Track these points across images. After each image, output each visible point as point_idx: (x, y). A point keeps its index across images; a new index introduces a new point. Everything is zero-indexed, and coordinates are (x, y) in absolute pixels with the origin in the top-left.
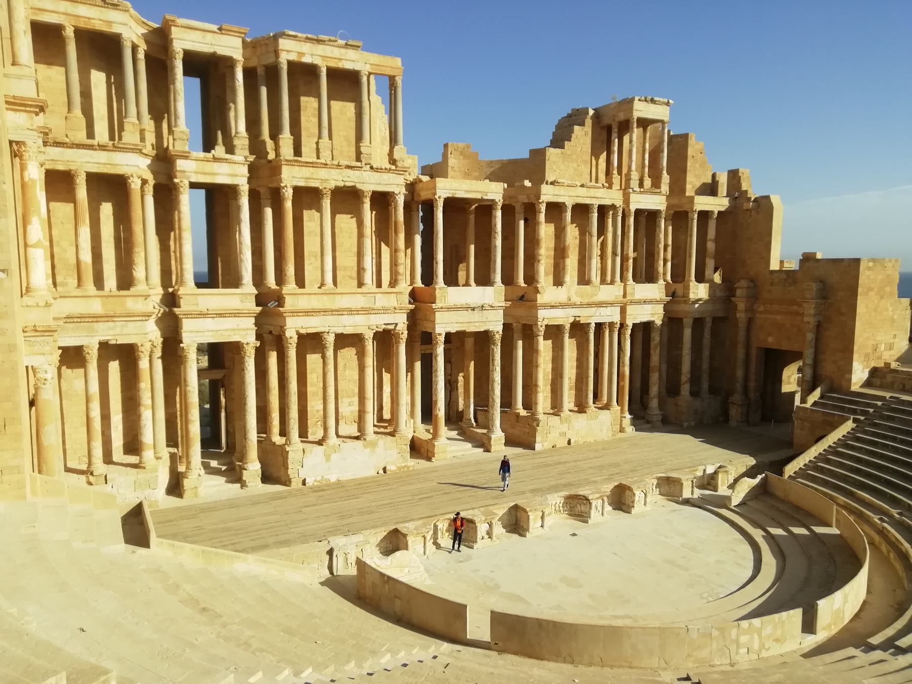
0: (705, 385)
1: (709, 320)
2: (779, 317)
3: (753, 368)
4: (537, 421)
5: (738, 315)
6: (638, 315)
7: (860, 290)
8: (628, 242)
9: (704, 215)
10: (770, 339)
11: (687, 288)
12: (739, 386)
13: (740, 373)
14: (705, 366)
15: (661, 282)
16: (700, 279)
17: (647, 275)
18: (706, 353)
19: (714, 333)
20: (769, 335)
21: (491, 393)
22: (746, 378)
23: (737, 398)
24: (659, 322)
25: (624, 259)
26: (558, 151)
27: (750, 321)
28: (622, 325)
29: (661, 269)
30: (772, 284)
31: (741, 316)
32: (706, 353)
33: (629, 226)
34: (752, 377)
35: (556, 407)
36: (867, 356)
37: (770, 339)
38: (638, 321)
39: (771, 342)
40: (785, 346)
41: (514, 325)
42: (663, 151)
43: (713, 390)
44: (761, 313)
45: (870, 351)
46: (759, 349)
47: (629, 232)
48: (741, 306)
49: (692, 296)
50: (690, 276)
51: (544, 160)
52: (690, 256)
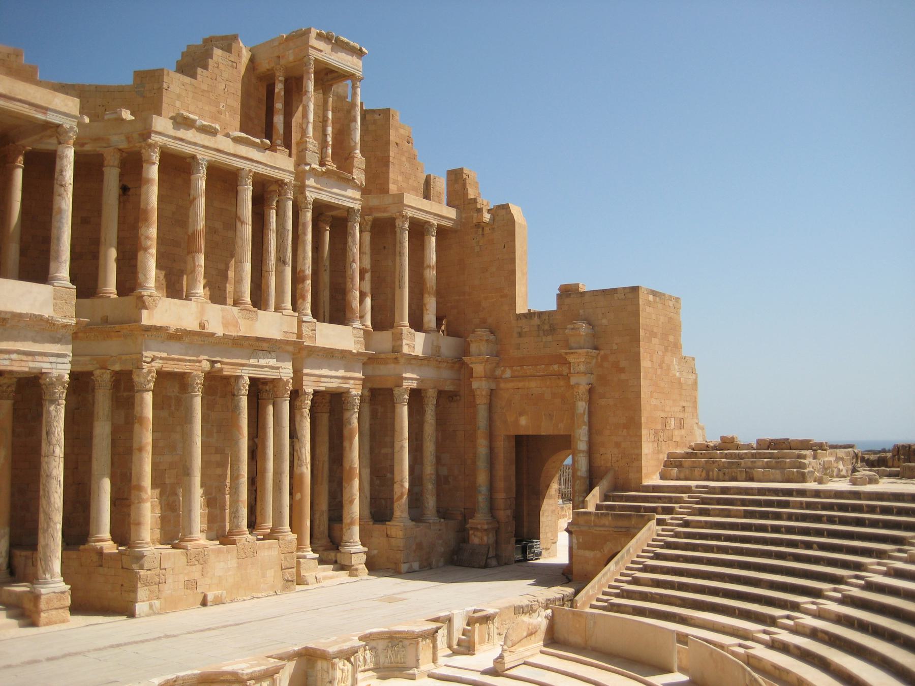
0: (431, 502)
1: (431, 394)
2: (533, 384)
3: (500, 471)
4: (140, 557)
5: (475, 385)
6: (321, 378)
7: (642, 333)
8: (304, 251)
9: (418, 230)
10: (523, 421)
11: (398, 338)
12: (482, 499)
13: (482, 479)
14: (429, 469)
15: (357, 324)
16: (417, 324)
17: (337, 313)
18: (429, 447)
19: (441, 421)
20: (521, 414)
21: (43, 502)
22: (492, 489)
23: (480, 519)
24: (356, 390)
25: (297, 279)
26: (187, 80)
27: (492, 393)
28: (296, 395)
29: (356, 304)
30: (520, 335)
31: (480, 386)
32: (429, 447)
33: (304, 225)
34: (500, 485)
35: (173, 533)
36: (656, 433)
37: (523, 421)
38: (322, 387)
39: (525, 424)
40: (546, 428)
41: (97, 372)
42: (355, 121)
43: (443, 513)
44: (507, 380)
45: (659, 426)
46: (508, 437)
47: (305, 234)
48: (479, 369)
49: (405, 350)
50: (402, 319)
51: (160, 90)
52: (401, 287)
